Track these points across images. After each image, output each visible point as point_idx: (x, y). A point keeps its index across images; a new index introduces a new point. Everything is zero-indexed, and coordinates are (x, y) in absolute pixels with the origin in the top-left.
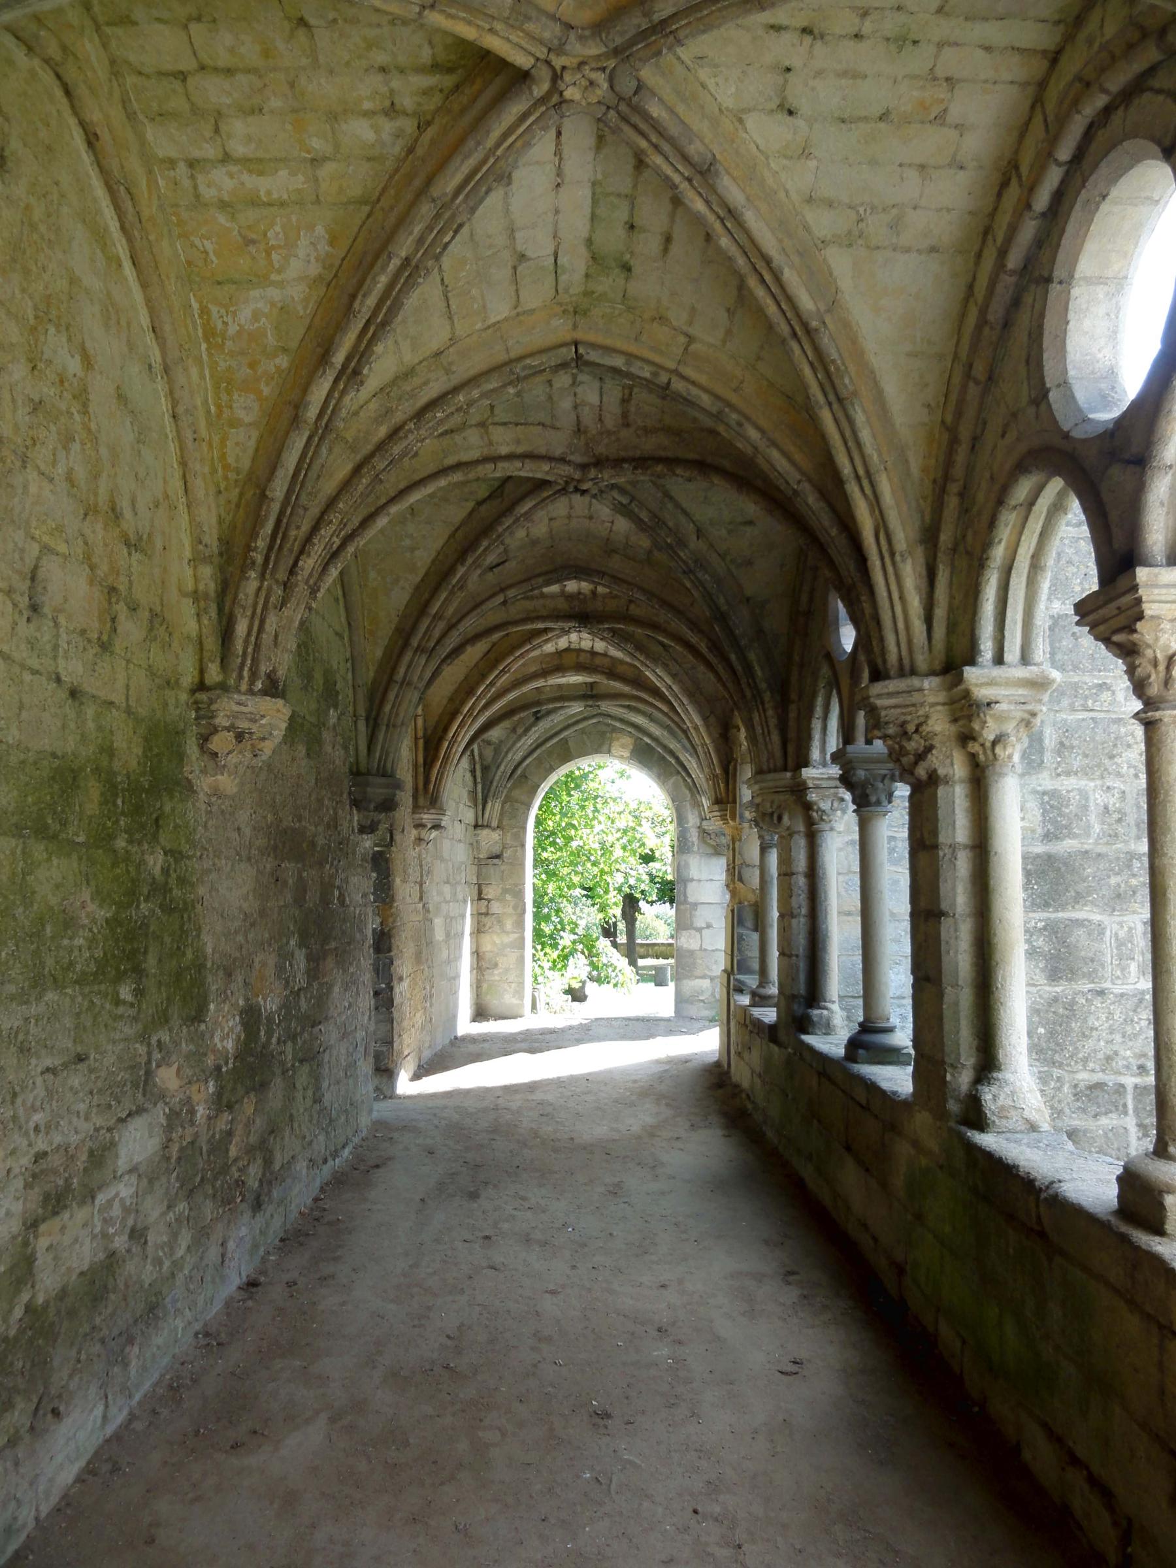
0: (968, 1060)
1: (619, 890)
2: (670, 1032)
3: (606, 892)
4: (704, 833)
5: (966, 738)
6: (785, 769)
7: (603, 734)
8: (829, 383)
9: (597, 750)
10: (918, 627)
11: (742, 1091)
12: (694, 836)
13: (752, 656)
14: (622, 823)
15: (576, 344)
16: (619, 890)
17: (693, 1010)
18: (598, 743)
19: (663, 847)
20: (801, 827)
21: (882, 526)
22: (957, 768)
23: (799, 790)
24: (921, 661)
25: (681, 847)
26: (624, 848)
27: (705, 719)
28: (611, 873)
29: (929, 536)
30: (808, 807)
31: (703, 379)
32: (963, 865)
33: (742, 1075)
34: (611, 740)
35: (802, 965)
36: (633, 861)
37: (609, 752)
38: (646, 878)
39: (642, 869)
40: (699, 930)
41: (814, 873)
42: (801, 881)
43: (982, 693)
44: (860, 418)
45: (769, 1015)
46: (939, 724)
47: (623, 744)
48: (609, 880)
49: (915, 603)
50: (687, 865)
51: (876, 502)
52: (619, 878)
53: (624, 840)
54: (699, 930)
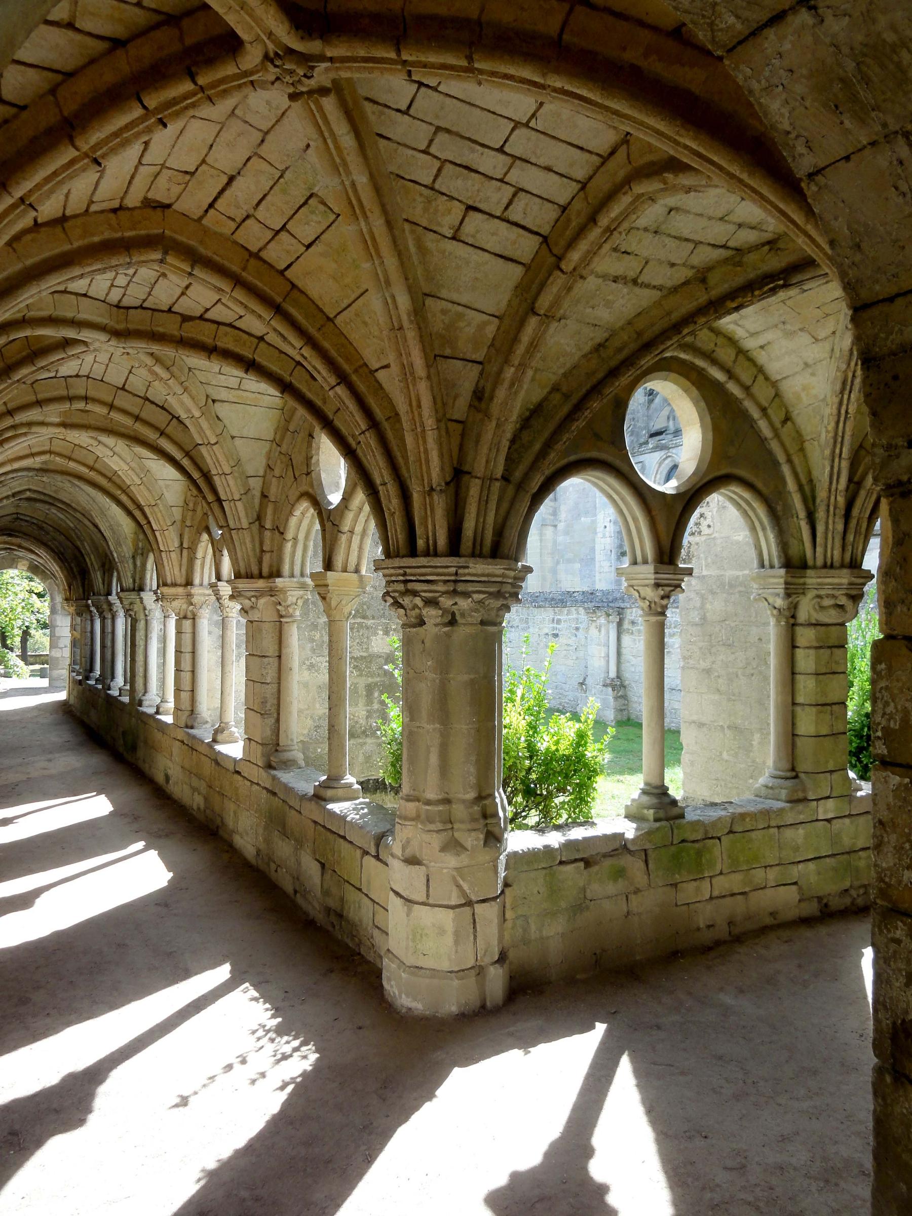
0: (110, 677)
1: (20, 628)
2: (46, 692)
3: (13, 629)
4: (63, 607)
5: (111, 610)
6: (84, 599)
7: (13, 559)
8: (78, 537)
9: (10, 567)
10: (101, 586)
11: (71, 705)
12: (59, 607)
13: (73, 565)
14: (22, 595)
15: (17, 513)
16: (20, 628)
17: (57, 683)
18: (12, 564)
19: (44, 606)
20: (89, 618)
21: (92, 564)
22: (109, 616)
23: (88, 606)
24: (102, 592)
25: (53, 611)
26: (23, 608)
27: (60, 568)
28: (15, 620)
29: (103, 565)
30: (91, 612)
31: (50, 523)
32: (110, 636)
33: (72, 702)
34: (17, 562)
35: (88, 661)
36: (28, 614)
37: (16, 568)
38: (35, 622)
39: (33, 618)
40: (61, 648)
41: (92, 632)
42: (89, 634)
43: (113, 602)
44: (86, 544)
45: (80, 678)
46: (105, 606)
47: (23, 565)
48: (14, 622)
49: (100, 580)
50: (55, 620)
51: (90, 559)
52: (19, 622)
53: (23, 604)
54: (61, 648)
